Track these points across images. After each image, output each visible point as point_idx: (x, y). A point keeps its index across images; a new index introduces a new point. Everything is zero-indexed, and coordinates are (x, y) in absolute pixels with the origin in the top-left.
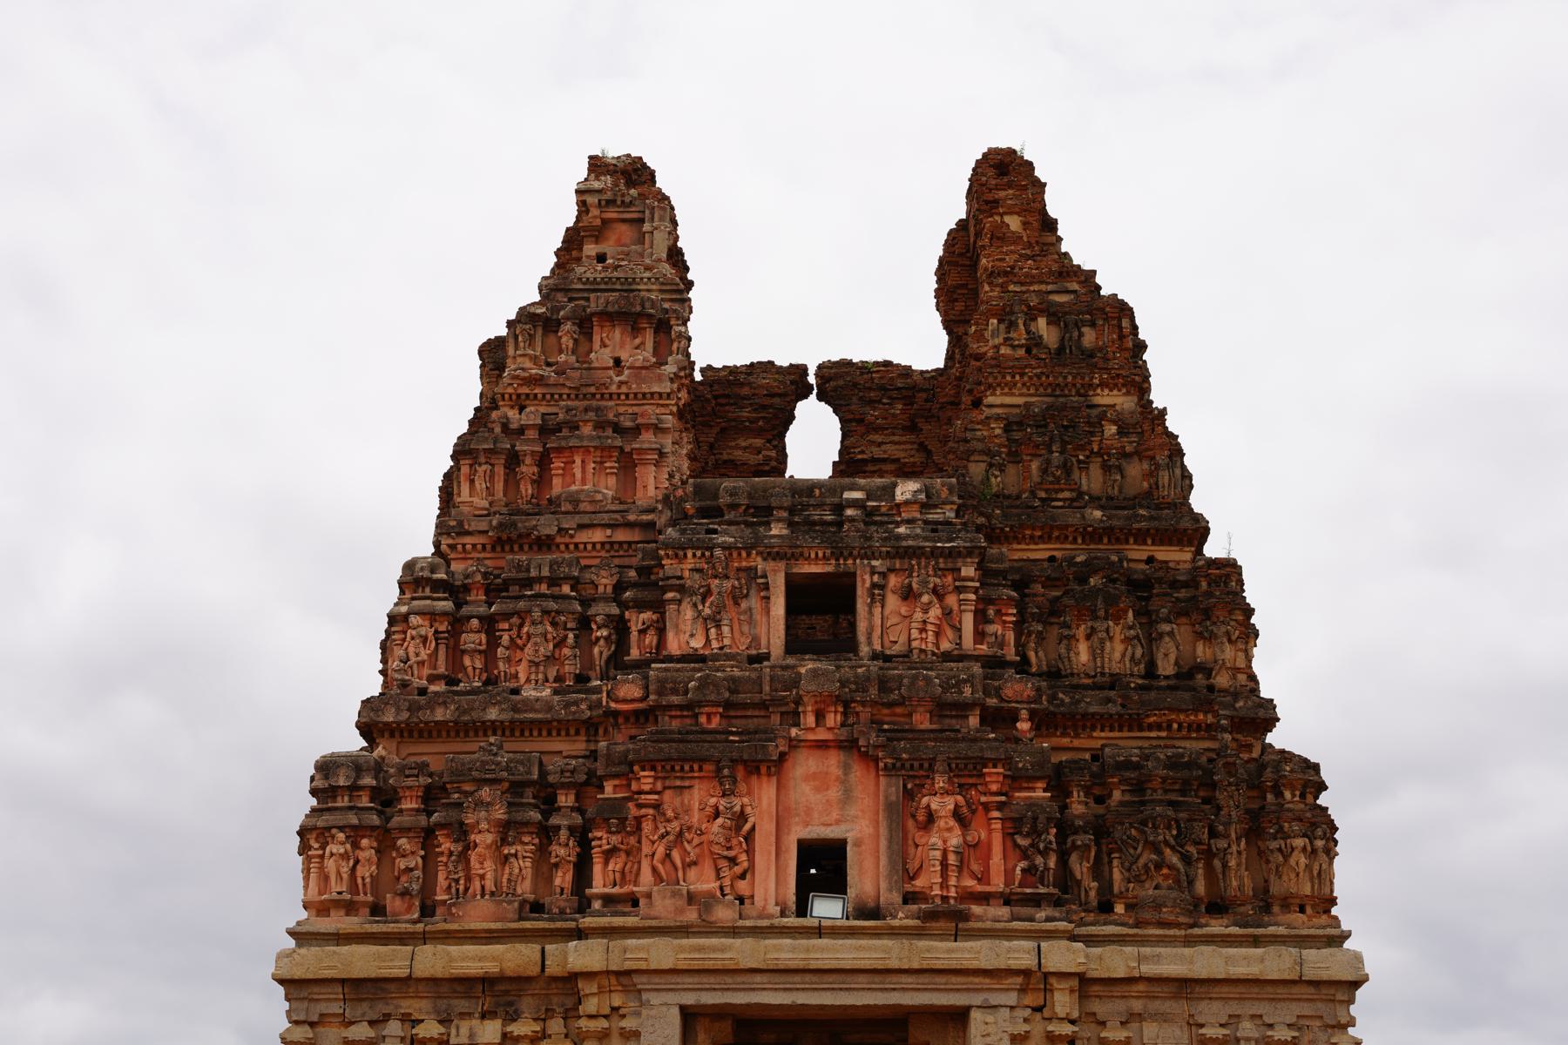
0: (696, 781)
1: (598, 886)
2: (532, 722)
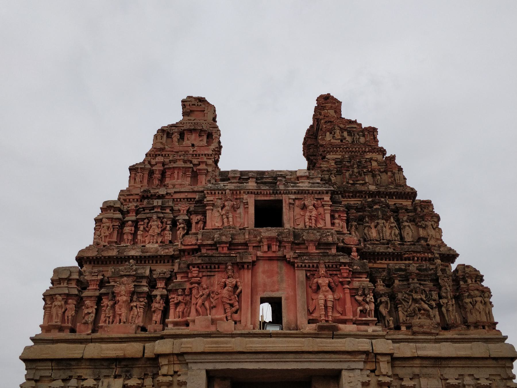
0: (217, 273)
1: (171, 318)
2: (149, 256)
